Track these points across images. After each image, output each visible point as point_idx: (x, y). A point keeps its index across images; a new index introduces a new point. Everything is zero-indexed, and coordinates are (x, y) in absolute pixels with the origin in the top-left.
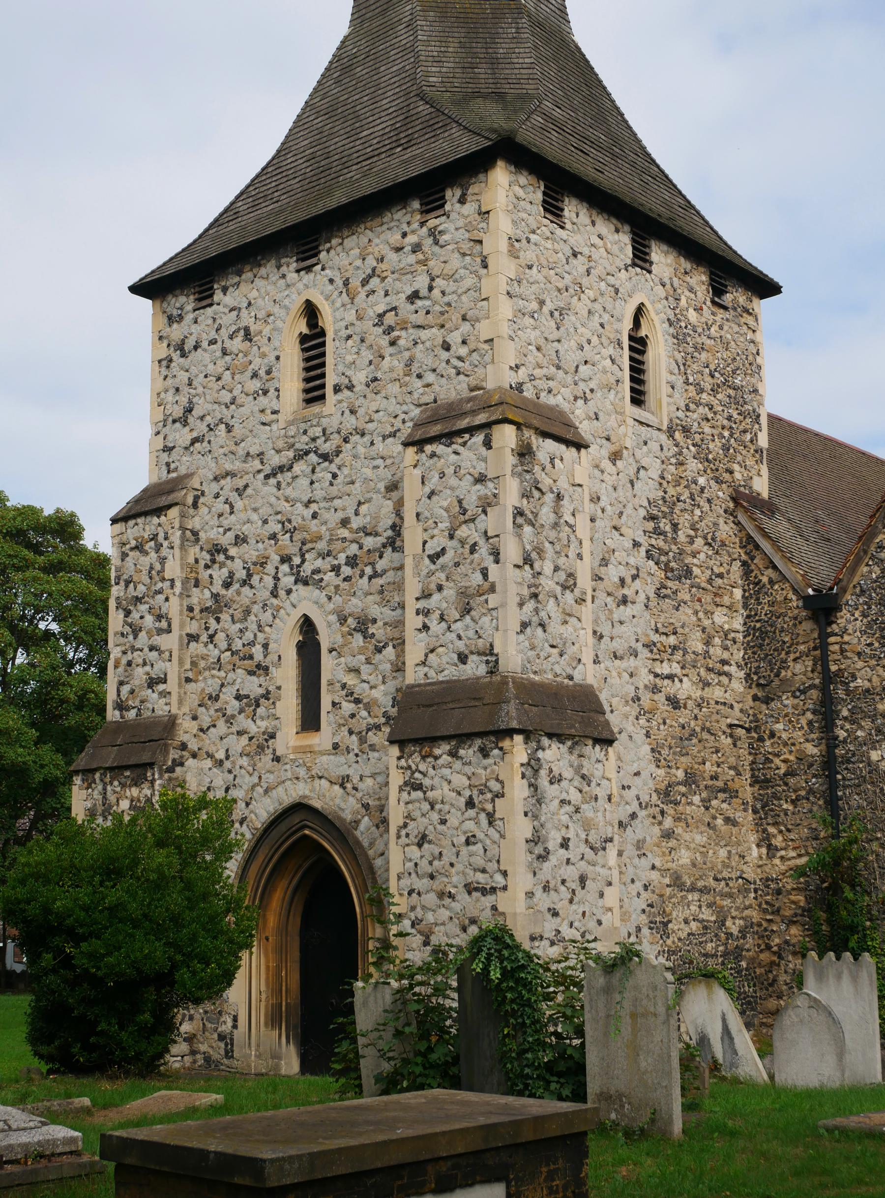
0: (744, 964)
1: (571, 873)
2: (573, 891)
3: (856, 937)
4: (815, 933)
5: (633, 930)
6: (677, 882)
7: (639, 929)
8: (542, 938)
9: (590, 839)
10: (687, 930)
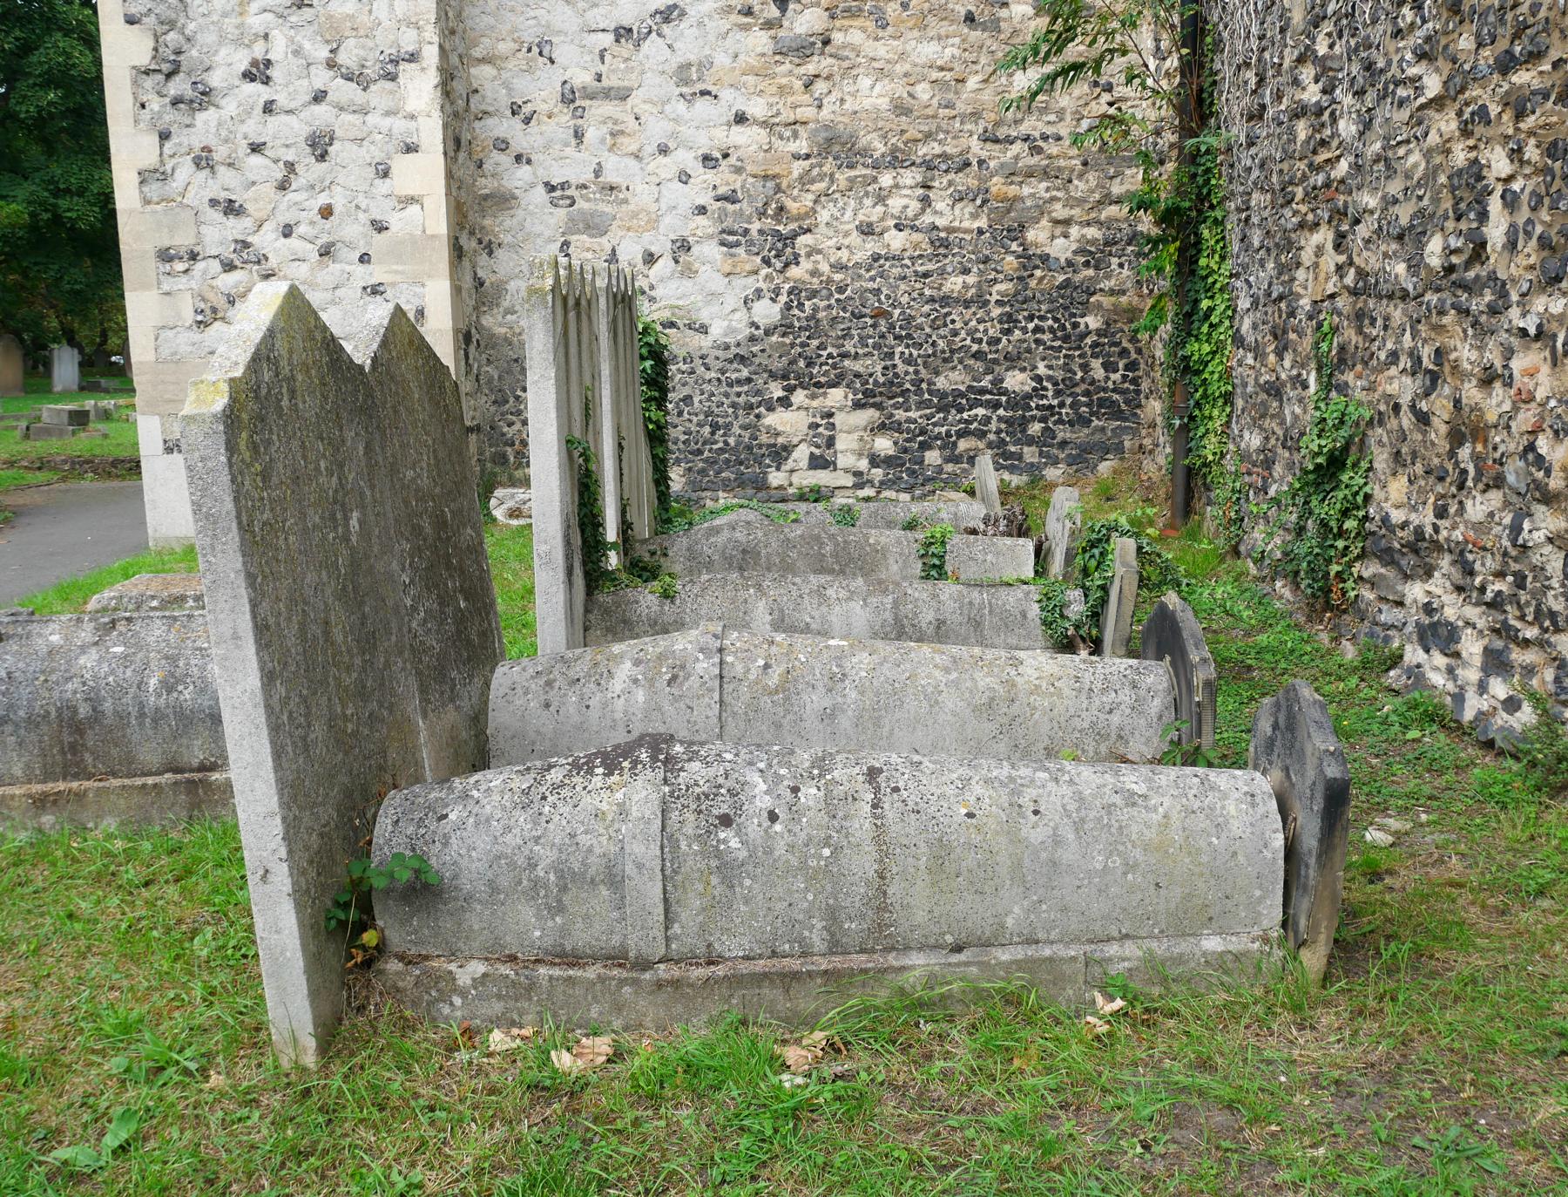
0: (1093, 322)
1: (287, 132)
2: (291, 167)
5: (661, 246)
6: (837, 146)
7: (683, 246)
8: (193, 257)
9: (342, 58)
10: (872, 246)
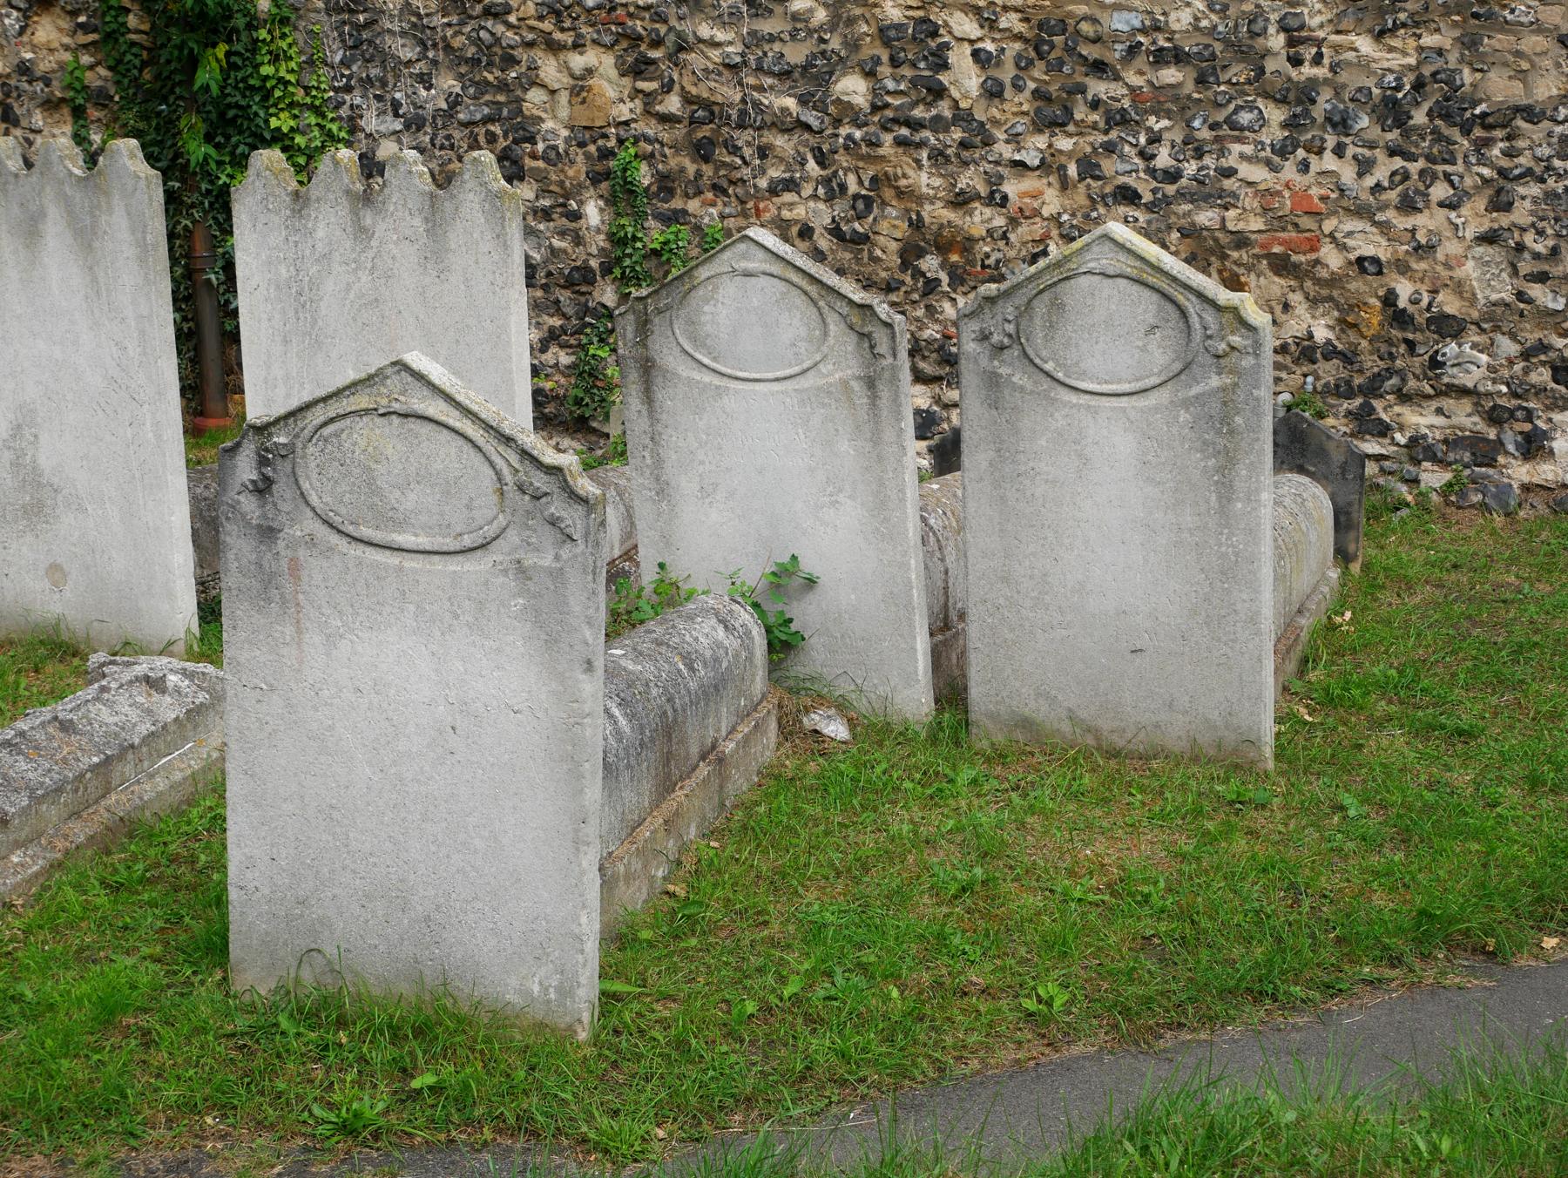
3: (221, 50)
4: (108, 39)
